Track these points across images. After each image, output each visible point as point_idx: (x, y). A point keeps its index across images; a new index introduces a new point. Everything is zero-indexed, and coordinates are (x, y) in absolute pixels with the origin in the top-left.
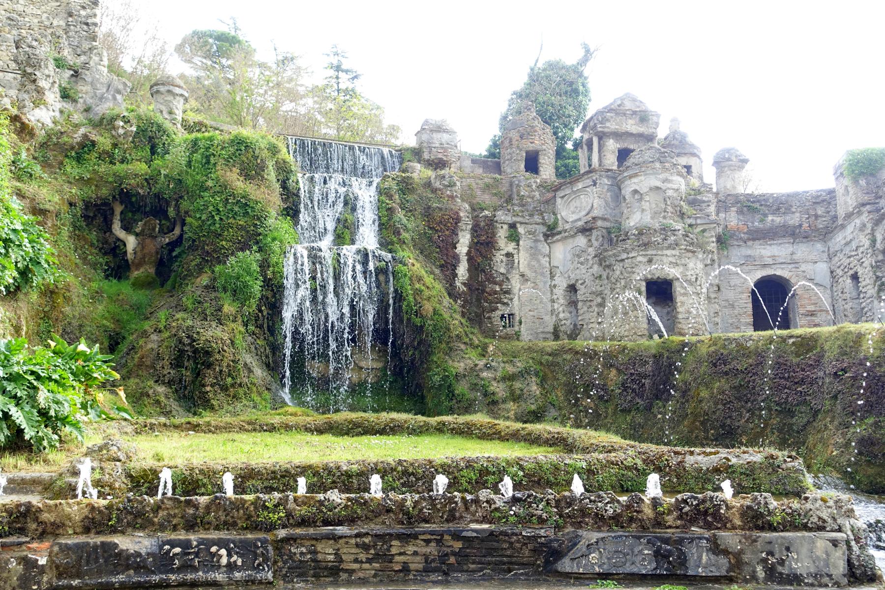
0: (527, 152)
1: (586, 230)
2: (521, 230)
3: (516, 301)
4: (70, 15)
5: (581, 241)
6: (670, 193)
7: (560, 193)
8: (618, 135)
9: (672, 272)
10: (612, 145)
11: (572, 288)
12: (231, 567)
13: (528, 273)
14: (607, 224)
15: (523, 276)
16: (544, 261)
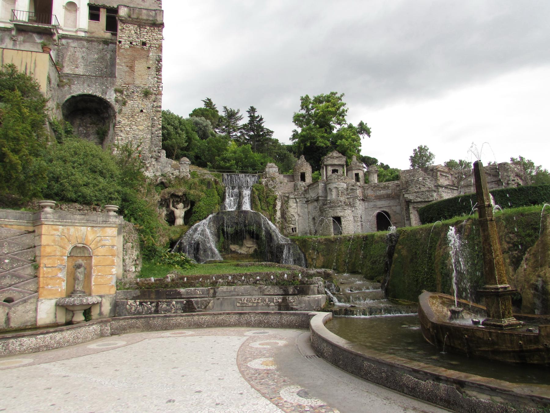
0: (301, 173)
1: (317, 200)
2: (298, 200)
3: (297, 224)
4: (152, 134)
5: (316, 204)
6: (340, 189)
7: (310, 188)
8: (332, 165)
9: (340, 214)
10: (330, 169)
11: (314, 219)
12: (200, 294)
13: (301, 214)
14: (322, 198)
15: (299, 215)
16: (306, 210)
